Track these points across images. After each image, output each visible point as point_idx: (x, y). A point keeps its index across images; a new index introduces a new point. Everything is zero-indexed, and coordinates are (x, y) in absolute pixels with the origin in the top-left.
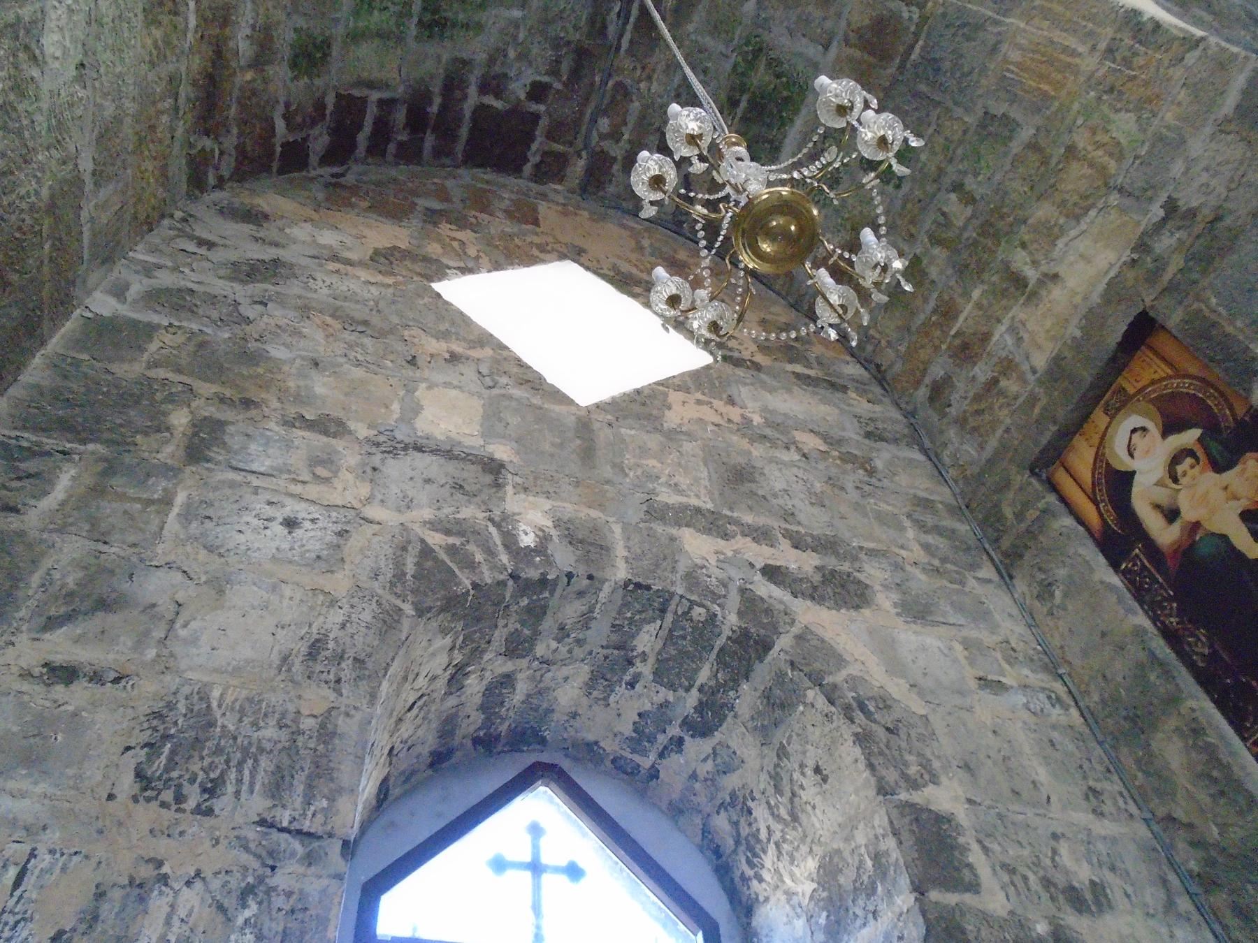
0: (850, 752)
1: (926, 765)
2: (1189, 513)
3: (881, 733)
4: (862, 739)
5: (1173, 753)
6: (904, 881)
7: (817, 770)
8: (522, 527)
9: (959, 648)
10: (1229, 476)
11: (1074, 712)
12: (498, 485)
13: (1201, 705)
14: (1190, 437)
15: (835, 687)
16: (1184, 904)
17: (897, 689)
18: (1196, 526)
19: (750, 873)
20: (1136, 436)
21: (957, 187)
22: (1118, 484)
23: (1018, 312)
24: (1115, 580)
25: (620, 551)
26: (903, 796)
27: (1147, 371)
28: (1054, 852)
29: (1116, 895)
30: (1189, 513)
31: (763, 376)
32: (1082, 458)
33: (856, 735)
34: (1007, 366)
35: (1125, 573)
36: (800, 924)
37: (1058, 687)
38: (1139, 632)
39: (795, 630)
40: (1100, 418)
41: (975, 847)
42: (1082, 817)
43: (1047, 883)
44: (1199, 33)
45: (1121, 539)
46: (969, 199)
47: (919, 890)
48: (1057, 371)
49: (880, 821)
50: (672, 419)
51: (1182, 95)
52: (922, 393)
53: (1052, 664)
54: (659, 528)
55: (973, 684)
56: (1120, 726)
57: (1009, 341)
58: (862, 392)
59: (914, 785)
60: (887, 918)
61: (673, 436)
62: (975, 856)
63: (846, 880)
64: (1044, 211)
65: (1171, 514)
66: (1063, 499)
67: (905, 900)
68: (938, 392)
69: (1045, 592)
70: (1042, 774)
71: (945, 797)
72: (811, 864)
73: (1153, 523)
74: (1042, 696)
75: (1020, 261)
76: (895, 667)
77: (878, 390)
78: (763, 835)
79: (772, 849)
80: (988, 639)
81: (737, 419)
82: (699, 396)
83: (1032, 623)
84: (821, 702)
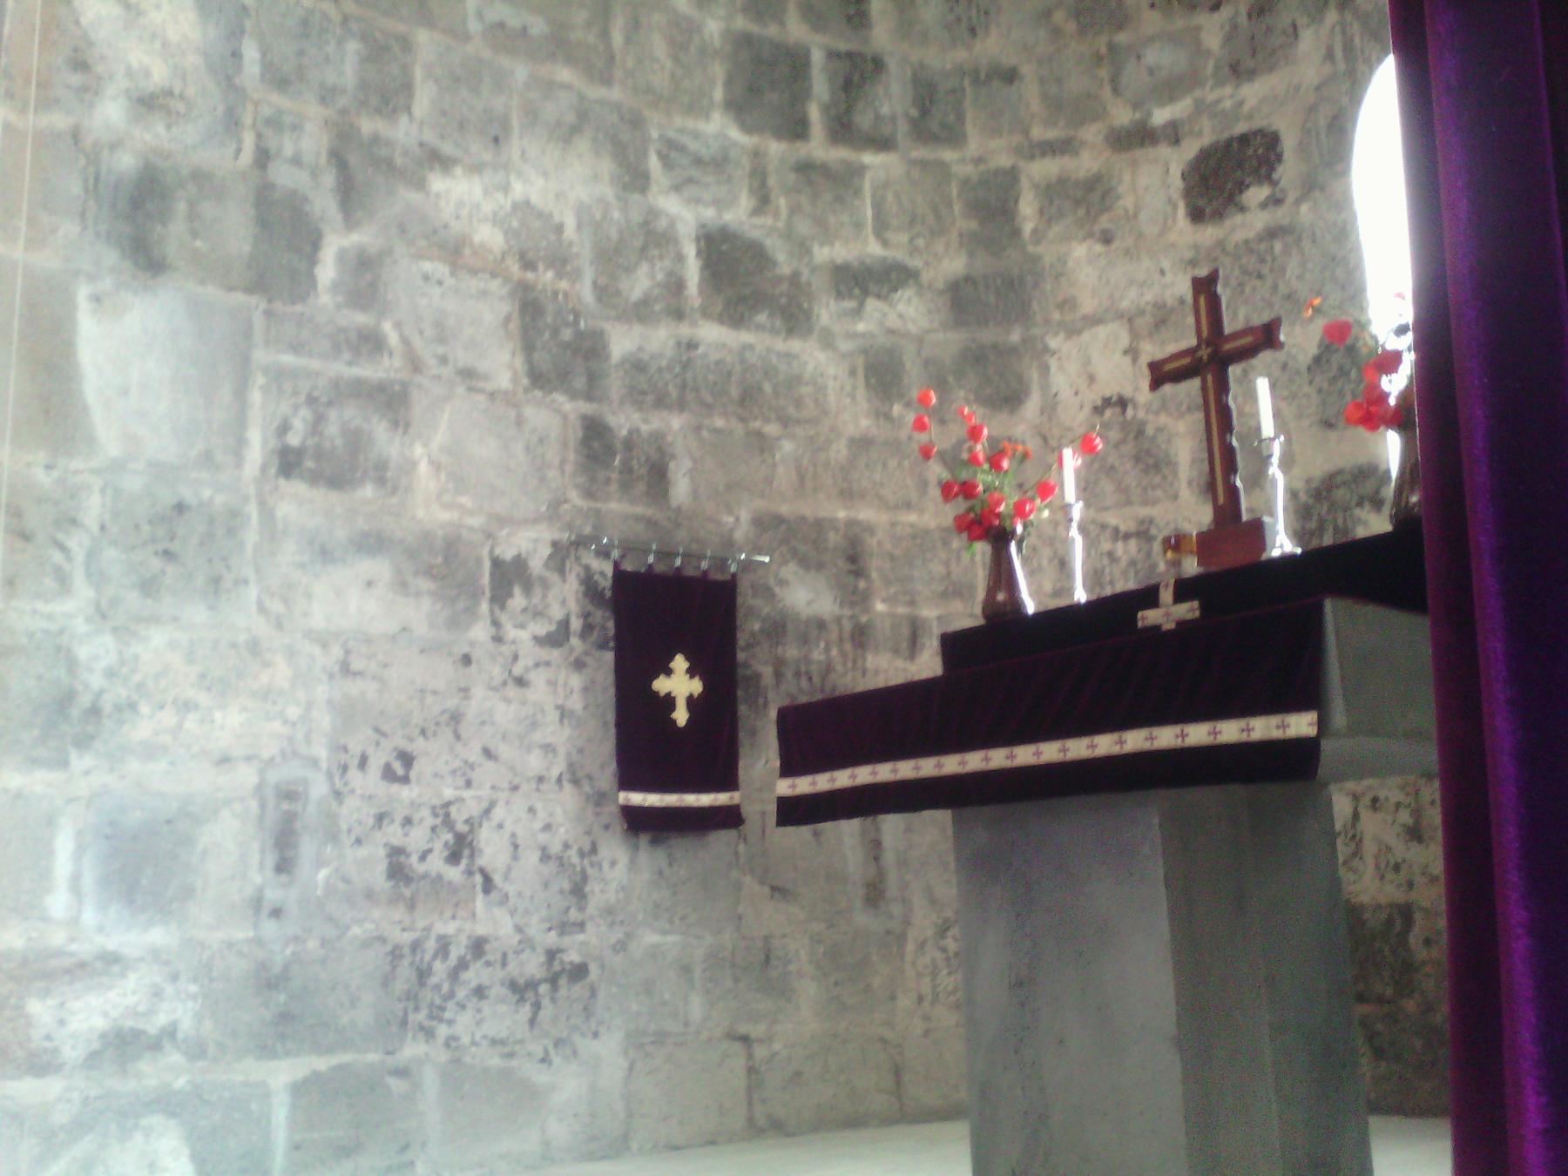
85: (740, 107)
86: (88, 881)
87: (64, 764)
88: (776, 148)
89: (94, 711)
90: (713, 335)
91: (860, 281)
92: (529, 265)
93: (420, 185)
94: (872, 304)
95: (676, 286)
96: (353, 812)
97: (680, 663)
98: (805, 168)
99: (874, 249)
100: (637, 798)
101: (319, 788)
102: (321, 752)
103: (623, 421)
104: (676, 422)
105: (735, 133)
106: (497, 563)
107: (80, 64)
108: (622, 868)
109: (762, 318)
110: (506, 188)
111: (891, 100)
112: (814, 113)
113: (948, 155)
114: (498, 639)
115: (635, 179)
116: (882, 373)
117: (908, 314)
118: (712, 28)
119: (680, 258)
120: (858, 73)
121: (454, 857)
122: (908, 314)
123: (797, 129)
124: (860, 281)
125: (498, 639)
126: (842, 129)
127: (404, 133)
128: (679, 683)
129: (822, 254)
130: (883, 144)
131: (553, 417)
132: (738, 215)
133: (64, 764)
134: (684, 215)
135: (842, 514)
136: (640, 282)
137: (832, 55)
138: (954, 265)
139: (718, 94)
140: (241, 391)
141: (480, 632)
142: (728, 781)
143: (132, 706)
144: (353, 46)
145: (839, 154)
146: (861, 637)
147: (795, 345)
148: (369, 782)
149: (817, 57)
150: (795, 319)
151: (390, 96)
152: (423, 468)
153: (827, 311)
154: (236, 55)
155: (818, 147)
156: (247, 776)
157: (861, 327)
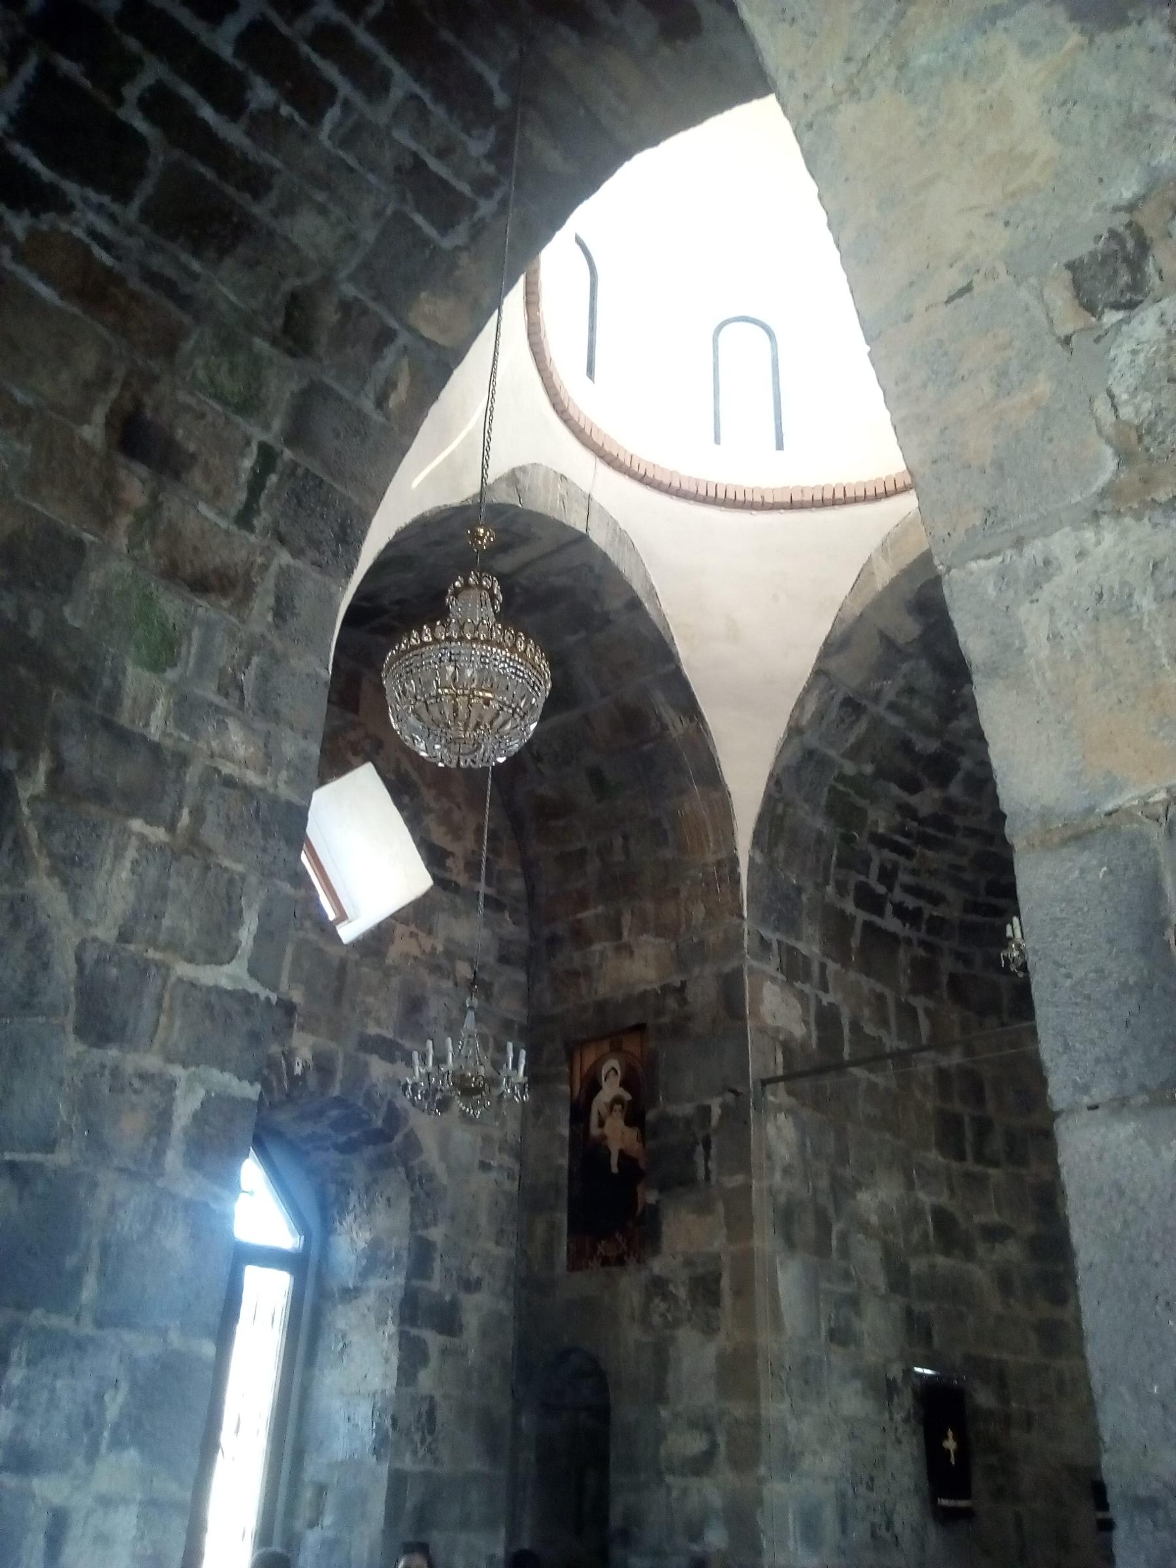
0: (405, 1204)
1: (435, 1216)
2: (607, 1130)
3: (422, 1194)
4: (414, 1201)
5: (540, 1229)
6: (404, 1273)
7: (388, 1199)
8: (298, 1060)
9: (479, 1140)
10: (627, 1129)
11: (517, 1183)
12: (291, 1026)
13: (562, 1218)
14: (627, 1097)
15: (412, 1168)
16: (510, 1290)
17: (440, 1169)
18: (604, 1137)
19: (337, 1217)
20: (612, 1072)
21: (626, 838)
22: (593, 1086)
23: (608, 946)
24: (566, 1132)
25: (339, 1076)
26: (420, 1232)
27: (632, 1045)
28: (470, 1262)
29: (485, 1284)
30: (607, 1130)
31: (458, 900)
32: (590, 1058)
33: (412, 1199)
34: (587, 973)
35: (571, 1130)
36: (353, 1258)
37: (517, 1167)
38: (560, 1167)
39: (406, 1130)
40: (606, 1046)
41: (438, 1260)
42: (490, 1246)
43: (459, 1277)
44: (745, 914)
45: (580, 1113)
46: (626, 851)
47: (408, 1278)
48: (601, 1006)
49: (405, 1242)
50: (393, 955)
51: (721, 935)
52: (545, 932)
53: (519, 1154)
54: (362, 1055)
55: (476, 1164)
56: (530, 1200)
57: (597, 960)
58: (514, 912)
59: (426, 1226)
60: (390, 1283)
61: (387, 973)
62: (437, 1265)
63: (381, 1254)
64: (650, 906)
65: (601, 1124)
66: (571, 1069)
67: (401, 1280)
68: (553, 942)
69: (538, 1112)
70: (483, 1219)
71: (436, 1234)
72: (368, 1236)
73: (594, 1119)
74: (505, 1174)
75: (627, 920)
76: (444, 1154)
77: (523, 907)
78: (351, 1207)
79: (352, 1216)
80: (496, 1134)
81: (428, 949)
82: (413, 928)
83: (523, 1126)
84: (403, 1175)
85: (941, 1146)
86: (798, 1535)
87: (787, 1480)
88: (955, 1165)
89: (793, 1455)
90: (940, 1260)
91: (994, 1234)
92: (886, 1233)
93: (854, 1197)
94: (997, 1246)
95: (925, 1236)
96: (860, 1504)
97: (950, 1433)
98: (967, 1175)
99: (996, 1217)
100: (944, 1502)
101: (850, 1493)
102: (848, 1475)
103: (918, 1307)
104: (930, 1307)
105: (940, 1159)
106: (888, 1380)
107: (769, 1157)
108: (934, 1536)
109: (956, 1252)
110: (876, 1196)
111: (997, 1144)
112: (969, 1149)
113: (1024, 1172)
114: (891, 1419)
115: (910, 1186)
116: (1004, 1281)
117: (1011, 1251)
118: (929, 1106)
119: (927, 1221)
120: (983, 1128)
121: (888, 1529)
122: (1011, 1251)
123: (961, 1157)
124: (994, 1234)
125: (891, 1419)
126: (980, 1158)
127: (848, 1172)
128: (950, 1444)
129: (978, 1219)
130: (996, 1164)
131: (896, 1305)
132: (944, 1200)
133: (787, 1480)
134: (925, 1199)
135: (995, 1356)
136: (915, 1236)
137: (973, 1119)
138: (1030, 1229)
139: (933, 1140)
140: (818, 1305)
141: (887, 1416)
142: (967, 1495)
143: (802, 1453)
144: (832, 1134)
145: (977, 1169)
146: (1007, 1420)
147: (970, 1266)
148: (862, 1490)
149: (967, 1119)
150: (969, 1254)
151: (842, 1157)
152: (866, 1336)
153: (981, 1249)
154: (804, 1145)
155: (970, 1165)
156: (831, 1487)
157: (995, 1257)
